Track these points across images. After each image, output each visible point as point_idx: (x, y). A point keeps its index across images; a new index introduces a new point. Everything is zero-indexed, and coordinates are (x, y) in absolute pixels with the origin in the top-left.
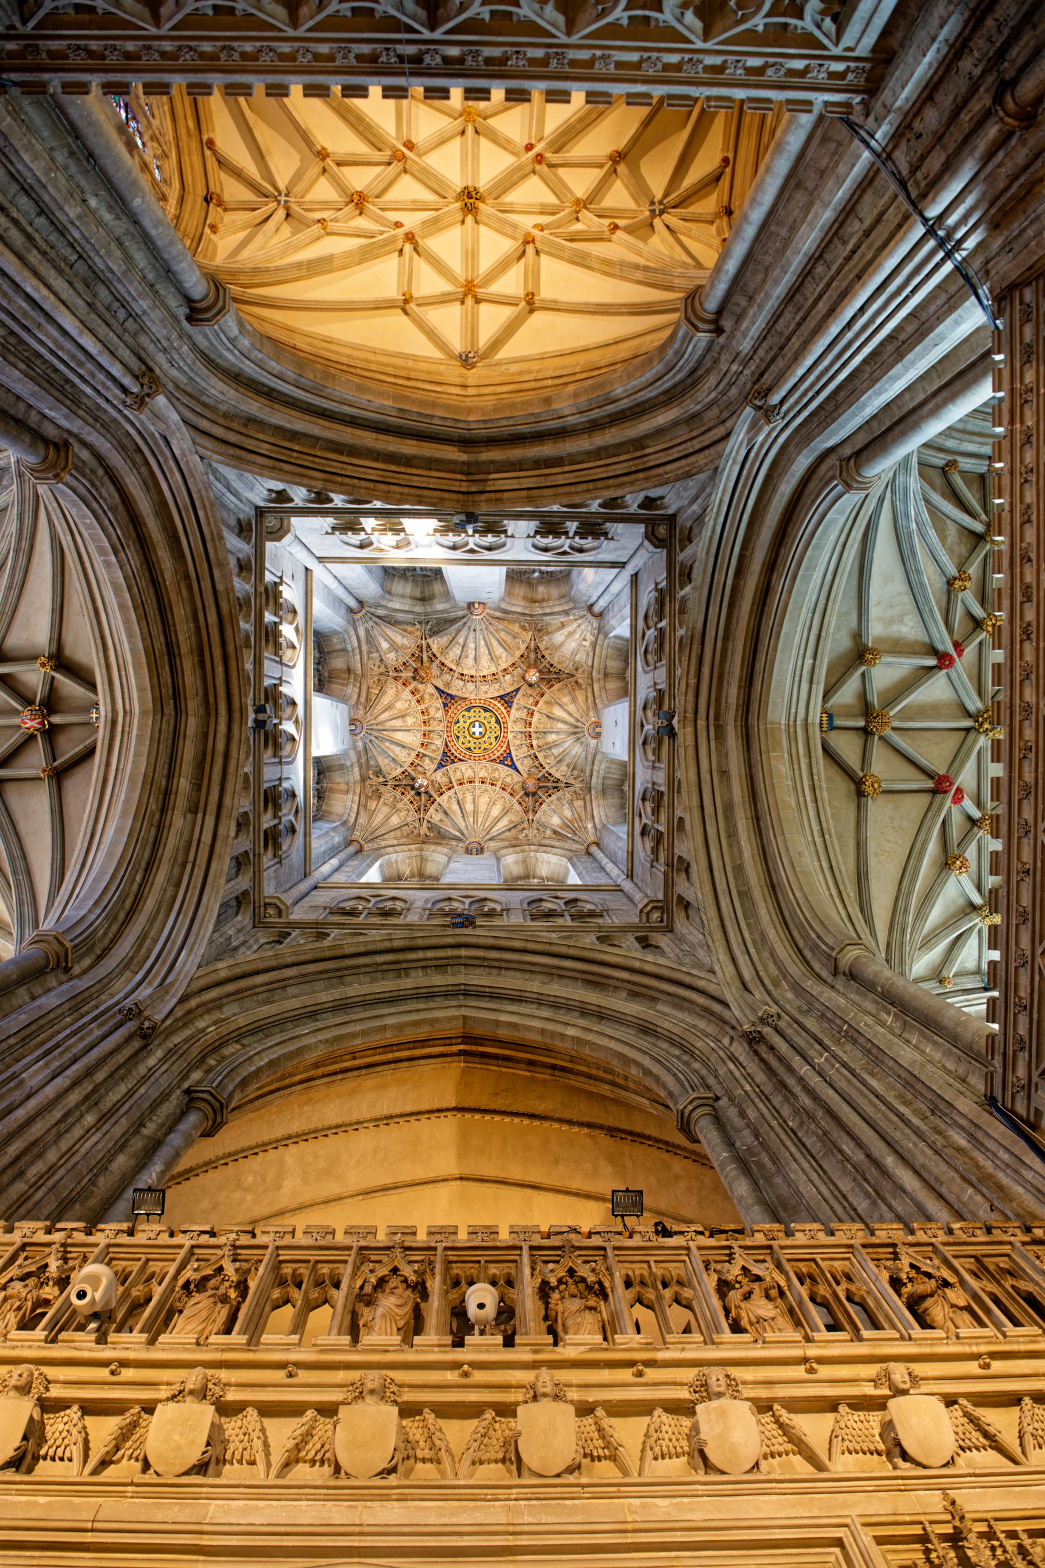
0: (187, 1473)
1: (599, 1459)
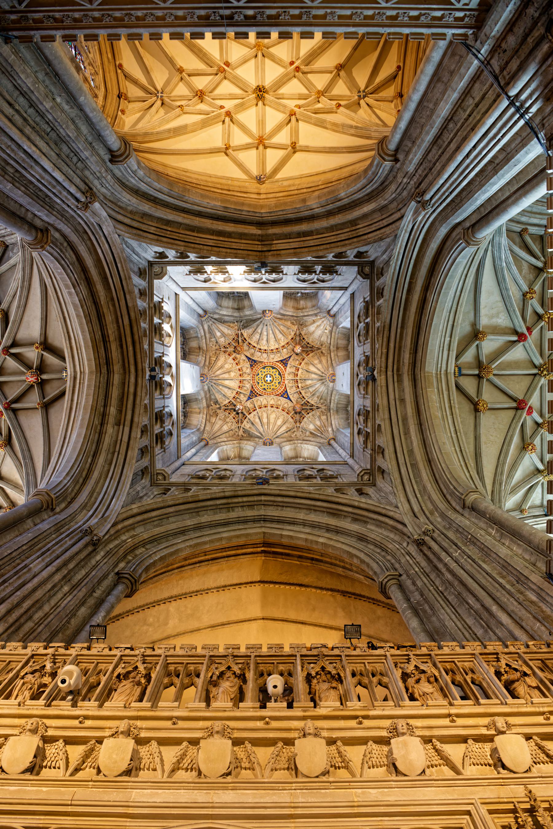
0: (120, 775)
1: (339, 768)
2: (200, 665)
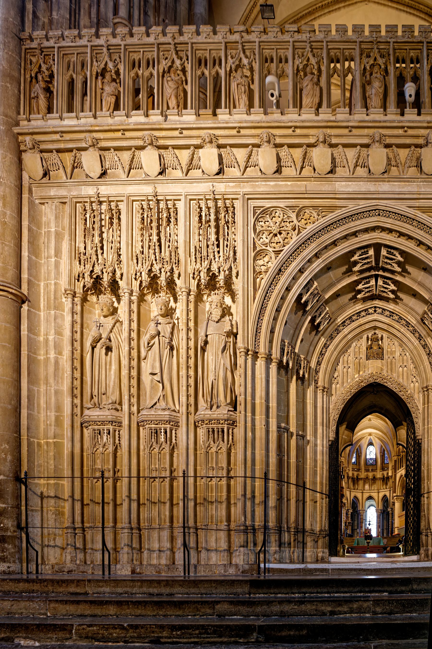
0: (328, 173)
2: (353, 51)
